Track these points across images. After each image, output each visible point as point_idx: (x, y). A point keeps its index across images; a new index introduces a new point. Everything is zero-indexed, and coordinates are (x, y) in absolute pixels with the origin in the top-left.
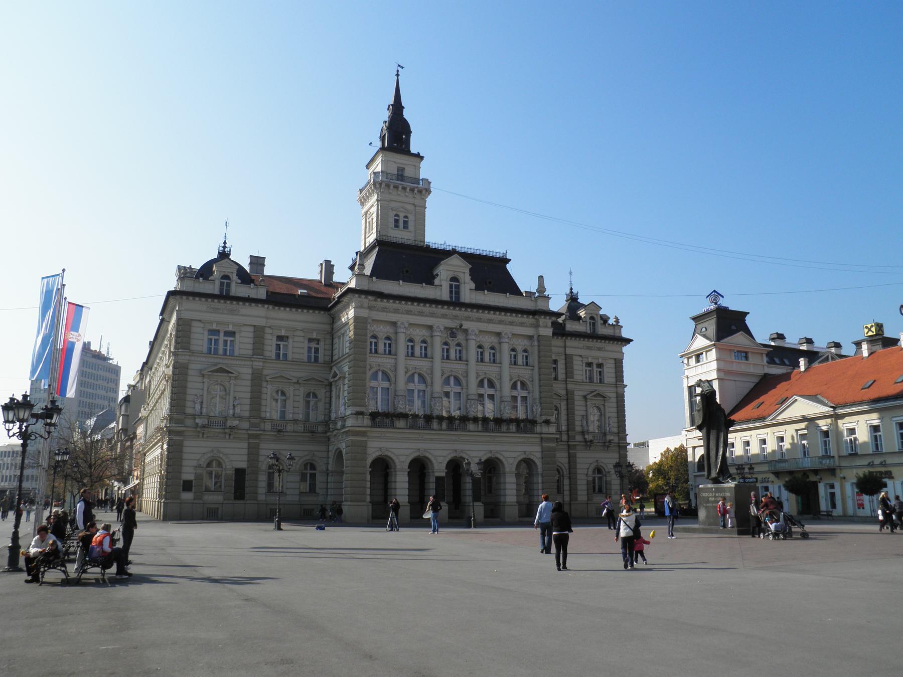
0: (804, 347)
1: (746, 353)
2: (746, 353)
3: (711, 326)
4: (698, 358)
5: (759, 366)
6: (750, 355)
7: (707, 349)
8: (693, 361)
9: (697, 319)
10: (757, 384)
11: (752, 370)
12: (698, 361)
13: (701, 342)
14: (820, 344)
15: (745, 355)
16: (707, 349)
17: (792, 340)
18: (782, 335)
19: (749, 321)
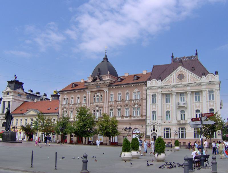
0: (38, 95)
1: (21, 94)
2: (21, 94)
3: (13, 85)
4: (8, 93)
5: (24, 98)
6: (22, 95)
7: (11, 92)
8: (6, 95)
9: (9, 82)
10: (22, 104)
11: (22, 99)
12: (7, 95)
13: (9, 90)
14: (42, 94)
15: (20, 95)
16: (11, 92)
17: (34, 92)
18: (32, 91)
19: (23, 85)
